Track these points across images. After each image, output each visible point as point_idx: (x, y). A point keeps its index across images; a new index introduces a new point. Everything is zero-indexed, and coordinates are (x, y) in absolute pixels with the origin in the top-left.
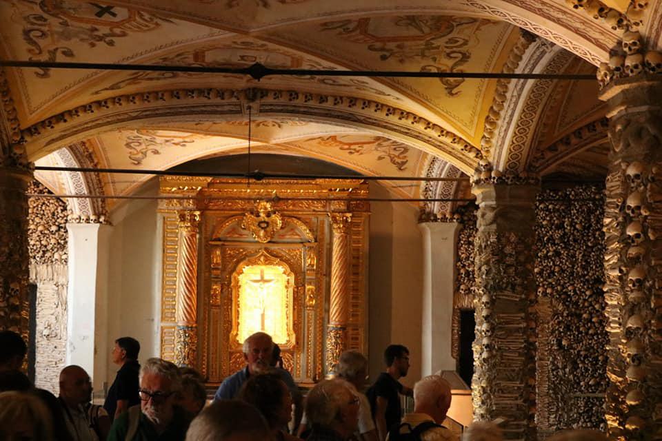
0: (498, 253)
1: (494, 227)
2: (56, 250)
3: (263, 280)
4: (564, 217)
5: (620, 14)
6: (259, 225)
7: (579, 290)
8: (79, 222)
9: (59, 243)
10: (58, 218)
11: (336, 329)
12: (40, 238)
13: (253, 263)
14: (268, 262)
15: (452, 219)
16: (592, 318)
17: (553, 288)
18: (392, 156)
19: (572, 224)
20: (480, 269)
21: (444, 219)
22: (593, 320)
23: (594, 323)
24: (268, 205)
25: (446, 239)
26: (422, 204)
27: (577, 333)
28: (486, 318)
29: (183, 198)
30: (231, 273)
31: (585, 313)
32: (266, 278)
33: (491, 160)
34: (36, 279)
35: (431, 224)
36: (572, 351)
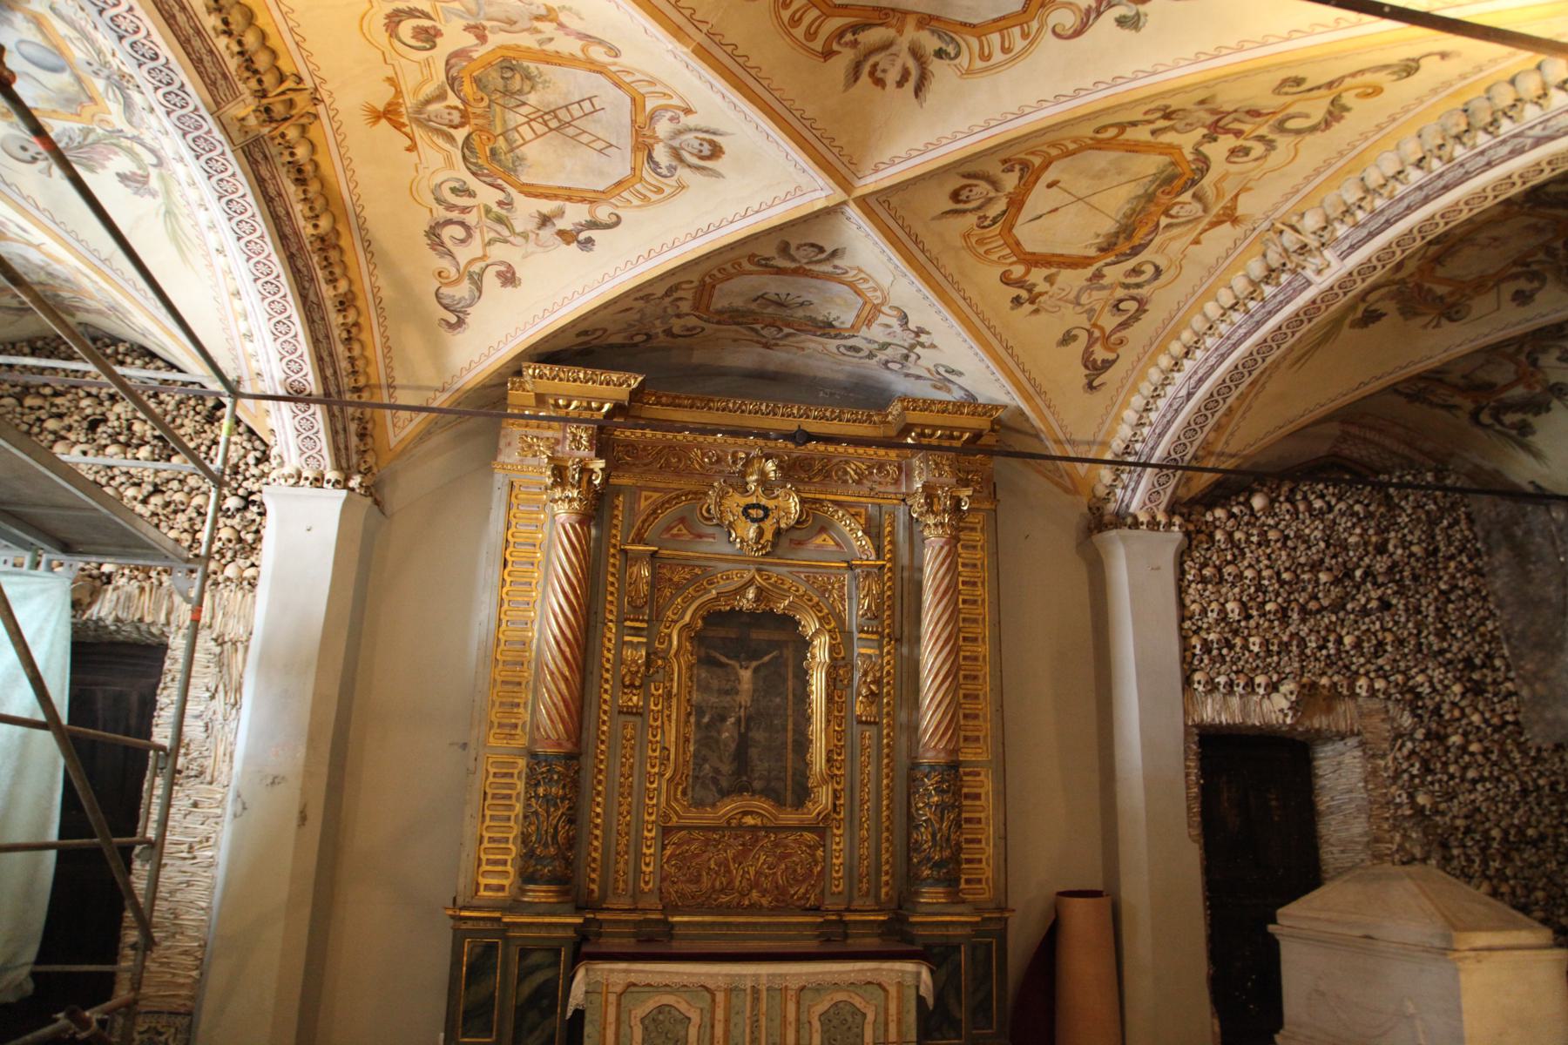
2: (229, 554)
4: (1387, 530)
7: (1441, 681)
8: (296, 484)
9: (240, 540)
10: (246, 479)
12: (192, 526)
15: (1170, 524)
16: (1468, 742)
17: (1386, 677)
18: (1097, 333)
19: (1404, 544)
21: (1153, 524)
22: (1474, 747)
23: (1472, 754)
24: (770, 466)
25: (1158, 568)
27: (1445, 778)
31: (1456, 733)
34: (168, 623)
35: (1125, 531)
36: (1438, 818)
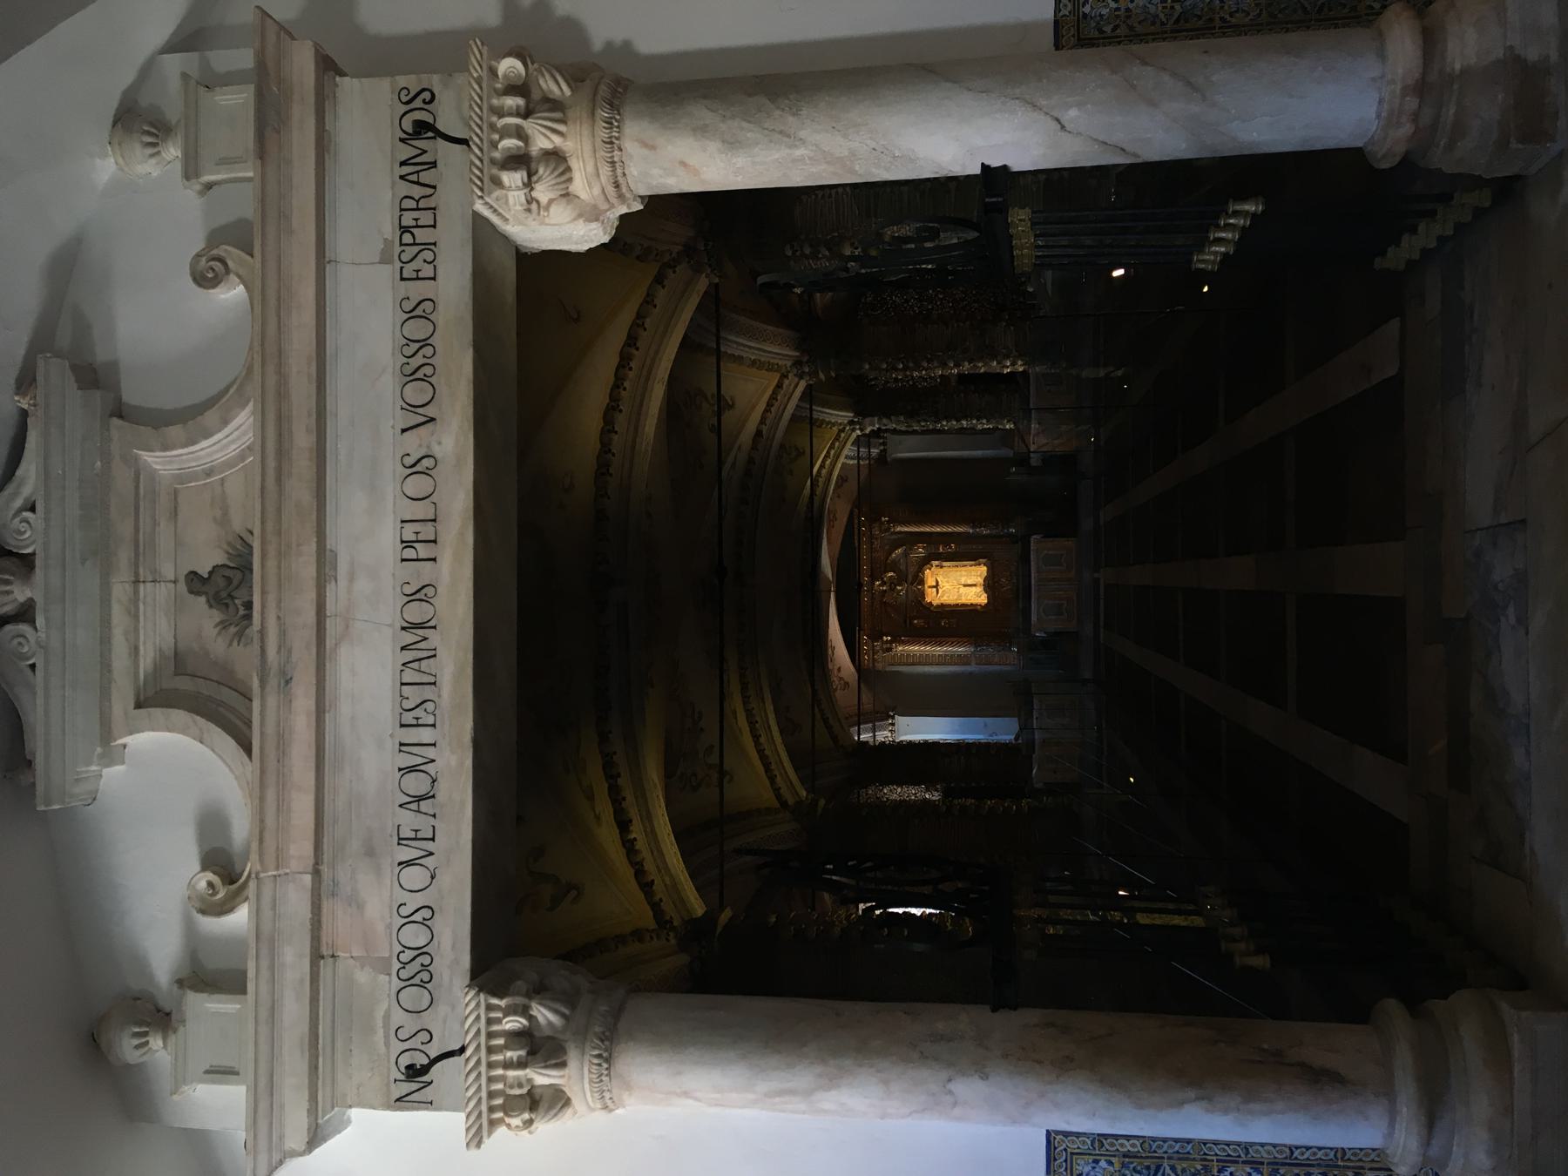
0: (912, 415)
1: (893, 417)
3: (937, 586)
5: (781, 377)
6: (893, 590)
11: (973, 528)
13: (923, 594)
14: (922, 582)
20: (924, 426)
21: (884, 444)
26: (872, 462)
28: (958, 421)
29: (873, 650)
30: (932, 611)
32: (934, 584)
33: (846, 422)
35: (887, 455)
